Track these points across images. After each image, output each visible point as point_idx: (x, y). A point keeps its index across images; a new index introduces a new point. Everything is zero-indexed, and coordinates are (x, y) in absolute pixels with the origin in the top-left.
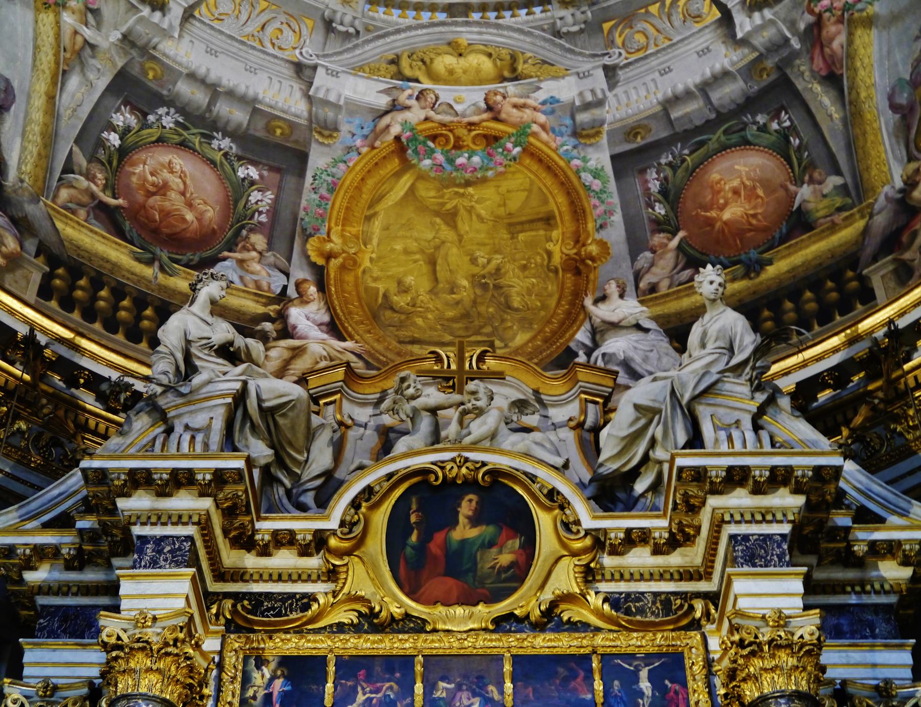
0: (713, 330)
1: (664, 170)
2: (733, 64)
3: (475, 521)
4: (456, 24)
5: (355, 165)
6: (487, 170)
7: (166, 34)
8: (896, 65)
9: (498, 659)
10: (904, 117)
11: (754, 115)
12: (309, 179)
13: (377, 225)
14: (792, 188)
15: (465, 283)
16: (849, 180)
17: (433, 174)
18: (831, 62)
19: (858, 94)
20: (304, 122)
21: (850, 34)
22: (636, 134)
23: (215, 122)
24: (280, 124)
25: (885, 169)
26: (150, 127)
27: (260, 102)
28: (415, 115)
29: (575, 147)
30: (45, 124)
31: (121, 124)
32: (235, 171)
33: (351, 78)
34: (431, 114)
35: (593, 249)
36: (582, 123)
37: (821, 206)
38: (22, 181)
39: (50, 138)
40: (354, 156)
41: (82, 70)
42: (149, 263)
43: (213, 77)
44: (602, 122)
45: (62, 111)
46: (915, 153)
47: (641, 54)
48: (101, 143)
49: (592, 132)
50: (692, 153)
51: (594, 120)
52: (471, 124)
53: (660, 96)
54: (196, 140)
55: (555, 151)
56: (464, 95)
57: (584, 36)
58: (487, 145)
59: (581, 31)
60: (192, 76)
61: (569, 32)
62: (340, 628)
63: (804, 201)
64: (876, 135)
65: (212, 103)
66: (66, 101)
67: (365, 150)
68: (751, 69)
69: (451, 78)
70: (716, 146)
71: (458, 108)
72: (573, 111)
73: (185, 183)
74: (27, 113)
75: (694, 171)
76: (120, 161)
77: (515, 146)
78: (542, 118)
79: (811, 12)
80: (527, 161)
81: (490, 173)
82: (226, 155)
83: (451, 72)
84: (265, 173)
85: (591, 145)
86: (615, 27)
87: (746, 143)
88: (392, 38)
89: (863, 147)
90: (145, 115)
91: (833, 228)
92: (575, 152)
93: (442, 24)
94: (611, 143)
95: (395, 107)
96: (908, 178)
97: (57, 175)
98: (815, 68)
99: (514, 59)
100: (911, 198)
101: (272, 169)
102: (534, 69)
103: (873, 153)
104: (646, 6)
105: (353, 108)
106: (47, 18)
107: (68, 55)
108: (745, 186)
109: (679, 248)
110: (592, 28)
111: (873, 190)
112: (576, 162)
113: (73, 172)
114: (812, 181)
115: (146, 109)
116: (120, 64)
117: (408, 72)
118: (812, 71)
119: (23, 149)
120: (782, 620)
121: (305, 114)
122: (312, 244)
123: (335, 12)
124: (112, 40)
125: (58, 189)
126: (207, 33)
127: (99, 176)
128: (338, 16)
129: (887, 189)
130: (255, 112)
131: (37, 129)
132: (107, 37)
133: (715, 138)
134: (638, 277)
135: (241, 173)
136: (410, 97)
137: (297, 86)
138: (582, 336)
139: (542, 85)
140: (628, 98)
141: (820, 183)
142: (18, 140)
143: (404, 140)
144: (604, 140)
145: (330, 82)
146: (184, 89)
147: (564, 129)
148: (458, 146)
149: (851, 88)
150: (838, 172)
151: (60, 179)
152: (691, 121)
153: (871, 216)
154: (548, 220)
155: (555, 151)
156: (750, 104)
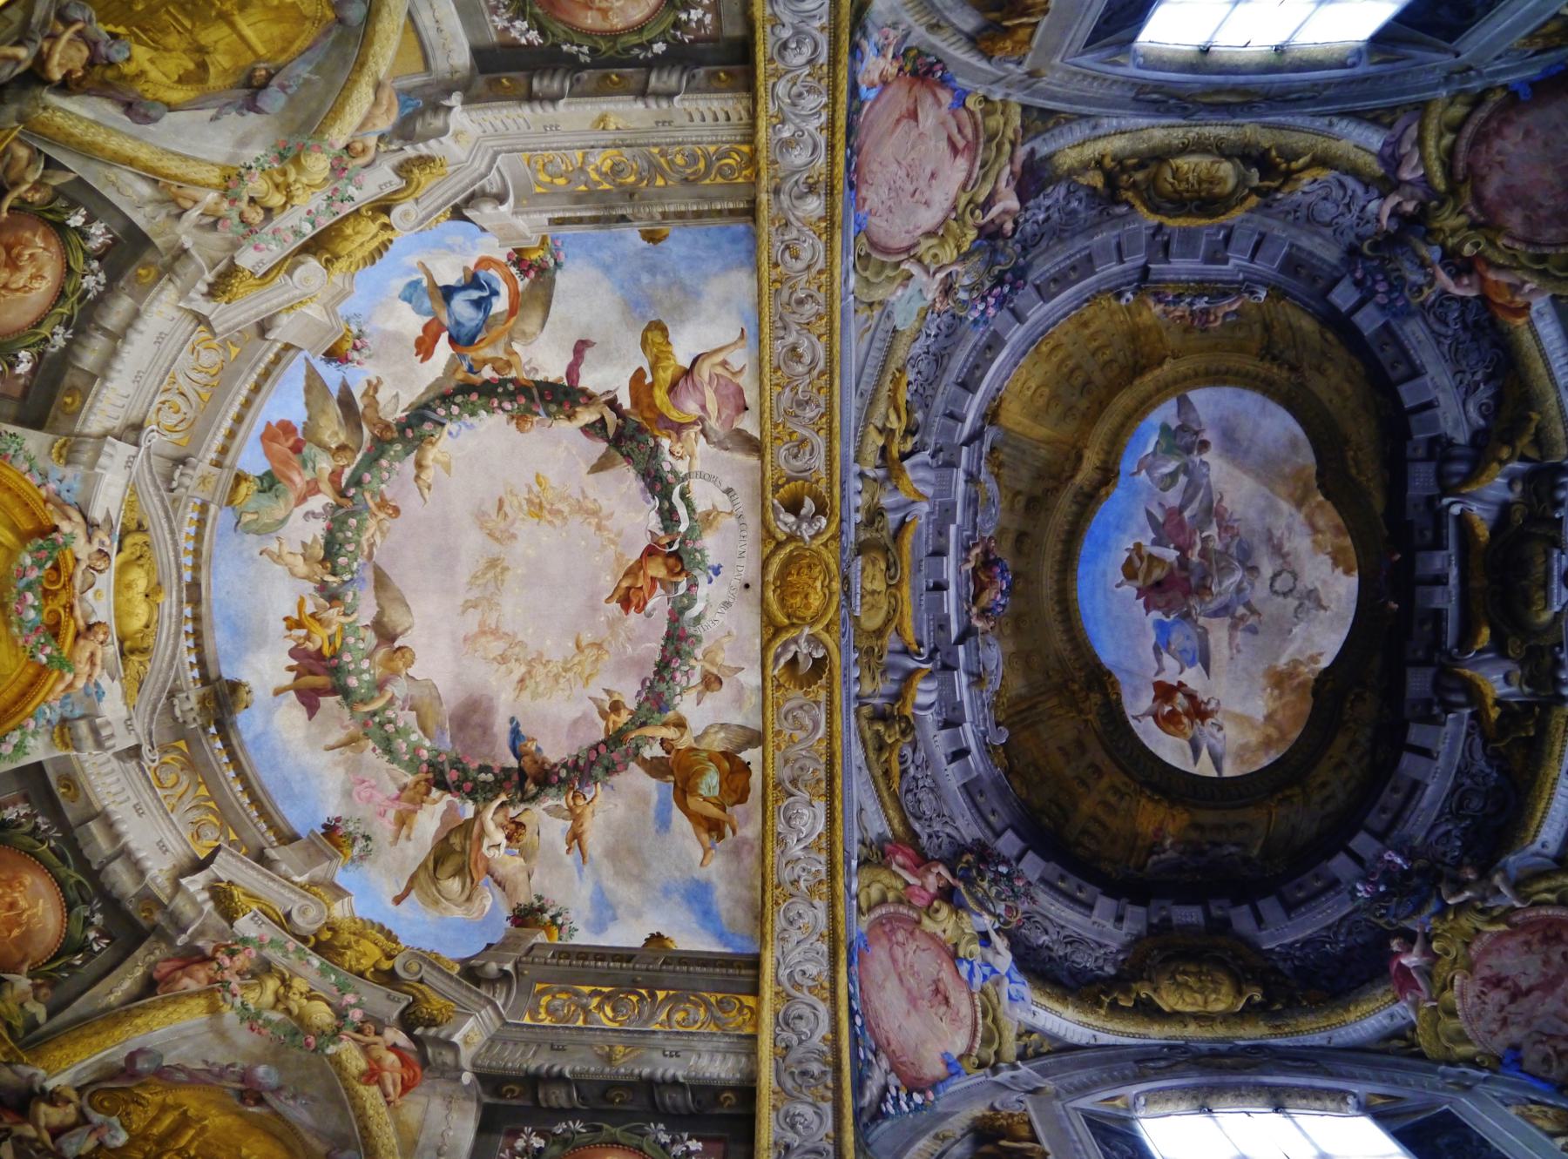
1: (29, 822)
2: (153, 879)
4: (180, 591)
5: (26, 481)
6: (20, 627)
7: (184, 294)
8: (176, 1048)
10: (123, 1070)
11: (100, 910)
12: (12, 429)
14: (25, 968)
16: (44, 1029)
17: (14, 567)
18: (169, 980)
19: (139, 1016)
20: (78, 428)
21: (198, 994)
22: (67, 787)
23: (84, 332)
24: (77, 403)
25: (63, 1066)
26: (86, 262)
27: (102, 384)
28: (81, 548)
29: (49, 721)
30: (103, 150)
31: (93, 231)
32: (26, 348)
33: (123, 482)
34: (83, 566)
36: (76, 728)
37: (10, 1004)
38: (45, 108)
39: (87, 151)
40: (38, 480)
41: (156, 201)
43: (133, 336)
44: (78, 749)
45: (116, 170)
46: (87, 1093)
47: (154, 782)
48: (74, 205)
49: (68, 739)
50: (52, 849)
51: (80, 740)
52: (72, 608)
53: (111, 808)
54: (65, 310)
55: (44, 700)
56: (104, 600)
57: (169, 722)
58: (48, 627)
59: (175, 719)
60: (136, 314)
61: (173, 706)
63: (12, 986)
64: (99, 1045)
65: (106, 332)
66: (125, 176)
67: (43, 492)
68: (149, 900)
69: (122, 586)
70: (63, 875)
71: (90, 594)
72: (89, 717)
73: (17, 290)
74: (119, 132)
75: (32, 855)
76: (51, 222)
77: (48, 656)
78: (80, 684)
79: (216, 950)
80: (31, 671)
81: (15, 630)
82: (46, 340)
83: (129, 586)
84: (22, 381)
85: (52, 739)
86: (182, 754)
87: (69, 906)
88: (166, 526)
89: (83, 1036)
90: (99, 259)
92: (42, 722)
93: (180, 577)
94: (55, 760)
95: (91, 526)
96: (58, 1094)
97: (45, 149)
98: (159, 965)
99: (144, 651)
100: (37, 1103)
101: (26, 389)
102: (134, 673)
103: (79, 1047)
104: (205, 782)
105: (91, 482)
106: (214, 177)
107: (174, 189)
108: (20, 915)
110: (179, 729)
111: (38, 1058)
112: (32, 724)
113: (46, 167)
114: (36, 987)
115: (107, 259)
116: (158, 241)
117: (129, 541)
118: (156, 962)
119: (80, 119)
121: (87, 431)
123: (194, 468)
124: (184, 238)
125: (30, 147)
126: (180, 336)
127: (37, 196)
128: (190, 471)
129: (42, 1072)
130: (93, 377)
131: (100, 139)
132: (186, 233)
133: (71, 872)
135: (23, 354)
136: (102, 543)
137: (117, 424)
139: (116, 682)
140: (107, 774)
141: (36, 998)
142: (91, 116)
143: (54, 535)
144: (59, 752)
145: (120, 460)
146: (122, 305)
147: (69, 708)
148: (46, 594)
149: (143, 1007)
150: (51, 1014)
151: (40, 152)
152: (87, 844)
153: (8, 1064)
155: (44, 700)
156: (112, 904)
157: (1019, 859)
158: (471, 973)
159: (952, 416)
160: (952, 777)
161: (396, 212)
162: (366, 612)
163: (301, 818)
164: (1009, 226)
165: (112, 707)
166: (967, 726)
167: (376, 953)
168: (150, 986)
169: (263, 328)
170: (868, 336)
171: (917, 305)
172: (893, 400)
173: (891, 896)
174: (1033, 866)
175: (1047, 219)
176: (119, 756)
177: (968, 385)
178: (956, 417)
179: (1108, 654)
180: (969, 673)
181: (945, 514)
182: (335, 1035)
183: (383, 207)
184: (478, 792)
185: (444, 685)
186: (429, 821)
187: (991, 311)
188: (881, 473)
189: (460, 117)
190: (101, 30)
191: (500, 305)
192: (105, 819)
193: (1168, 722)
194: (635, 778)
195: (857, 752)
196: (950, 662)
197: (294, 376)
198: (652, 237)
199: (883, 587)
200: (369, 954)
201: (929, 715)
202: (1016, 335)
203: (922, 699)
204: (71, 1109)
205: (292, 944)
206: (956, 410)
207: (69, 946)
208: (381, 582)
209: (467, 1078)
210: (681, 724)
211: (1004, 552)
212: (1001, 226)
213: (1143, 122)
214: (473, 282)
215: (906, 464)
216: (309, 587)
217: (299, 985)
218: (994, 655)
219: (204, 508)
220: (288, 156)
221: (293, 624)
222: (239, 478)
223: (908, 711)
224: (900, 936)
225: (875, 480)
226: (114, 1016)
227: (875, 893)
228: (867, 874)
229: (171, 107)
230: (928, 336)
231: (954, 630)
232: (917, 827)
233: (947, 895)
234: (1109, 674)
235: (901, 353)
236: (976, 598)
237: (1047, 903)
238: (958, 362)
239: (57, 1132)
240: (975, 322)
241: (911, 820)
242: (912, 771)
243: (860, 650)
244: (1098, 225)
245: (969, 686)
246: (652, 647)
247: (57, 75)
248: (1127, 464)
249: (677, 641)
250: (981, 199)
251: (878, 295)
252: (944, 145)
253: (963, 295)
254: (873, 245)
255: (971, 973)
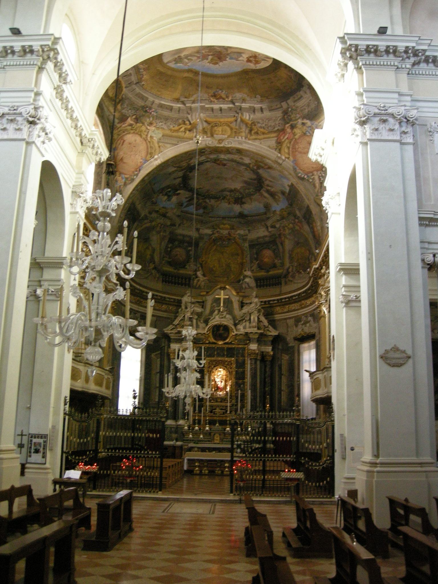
0: (255, 301)
3: (223, 330)
9: (224, 348)
13: (210, 255)
15: (224, 265)
28: (217, 235)
35: (245, 261)
39: (160, 253)
42: (175, 269)
60: (181, 235)
62: (207, 343)
68: (270, 237)
69: (222, 229)
72: (243, 236)
87: (269, 248)
91: (279, 269)
95: (213, 234)
105: (206, 234)
106: (159, 235)
109: (258, 264)
120: (254, 350)
122: (200, 259)
134: (251, 267)
138: (242, 277)
144: (247, 242)
148: (224, 240)
154: (238, 255)
157: (288, 105)
158: (291, 205)
159: (179, 111)
160: (267, 114)
161: (158, 209)
162: (228, 193)
163: (263, 210)
164: (134, 117)
165: (242, 232)
166: (255, 106)
167: (284, 213)
168: (282, 244)
169: (179, 216)
170: (166, 145)
171: (157, 131)
172: (177, 131)
173: (288, 145)
174: (290, 102)
175: (130, 109)
176: (249, 233)
177: (171, 109)
178: (179, 110)
179: (239, 69)
180: (242, 103)
181: (203, 108)
182: (294, 227)
183: (157, 212)
184: (262, 187)
185: (242, 185)
186: (266, 195)
187: (153, 110)
188: (195, 130)
189: (143, 215)
190: (147, 264)
191: (169, 190)
192: (259, 238)
193: (257, 62)
194: (261, 171)
195: (257, 143)
196: (239, 108)
197: (185, 209)
198: (154, 184)
199: (221, 127)
200: (285, 214)
201: (252, 116)
202: (157, 101)
203: (248, 118)
204: (291, 267)
205: (281, 222)
206: (178, 110)
207: (274, 251)
208: (223, 191)
209: (303, 220)
210: (250, 164)
211: (212, 92)
212: (135, 118)
213: (105, 108)
214: (166, 194)
215: (192, 122)
216: (223, 201)
217: (287, 225)
218: (238, 95)
219: (210, 217)
220: (153, 228)
221: (229, 203)
222: (204, 212)
223: (250, 123)
224: (297, 147)
225: (196, 132)
226: (284, 252)
227: (286, 151)
228: (282, 151)
229: (152, 247)
230: (162, 125)
231: (231, 106)
232: (276, 129)
233: (293, 127)
234: (244, 70)
235: (168, 132)
236: (224, 99)
237: (300, 104)
238: (166, 113)
239: (292, 271)
240: (156, 113)
241: (274, 130)
242: (264, 125)
243: (235, 136)
244: (128, 99)
245: (245, 103)
246: (234, 163)
247: (154, 265)
248: (186, 68)
249: (232, 160)
250: (130, 127)
251: (156, 145)
252: (124, 146)
253: (151, 119)
254: (147, 152)
255: (309, 133)
